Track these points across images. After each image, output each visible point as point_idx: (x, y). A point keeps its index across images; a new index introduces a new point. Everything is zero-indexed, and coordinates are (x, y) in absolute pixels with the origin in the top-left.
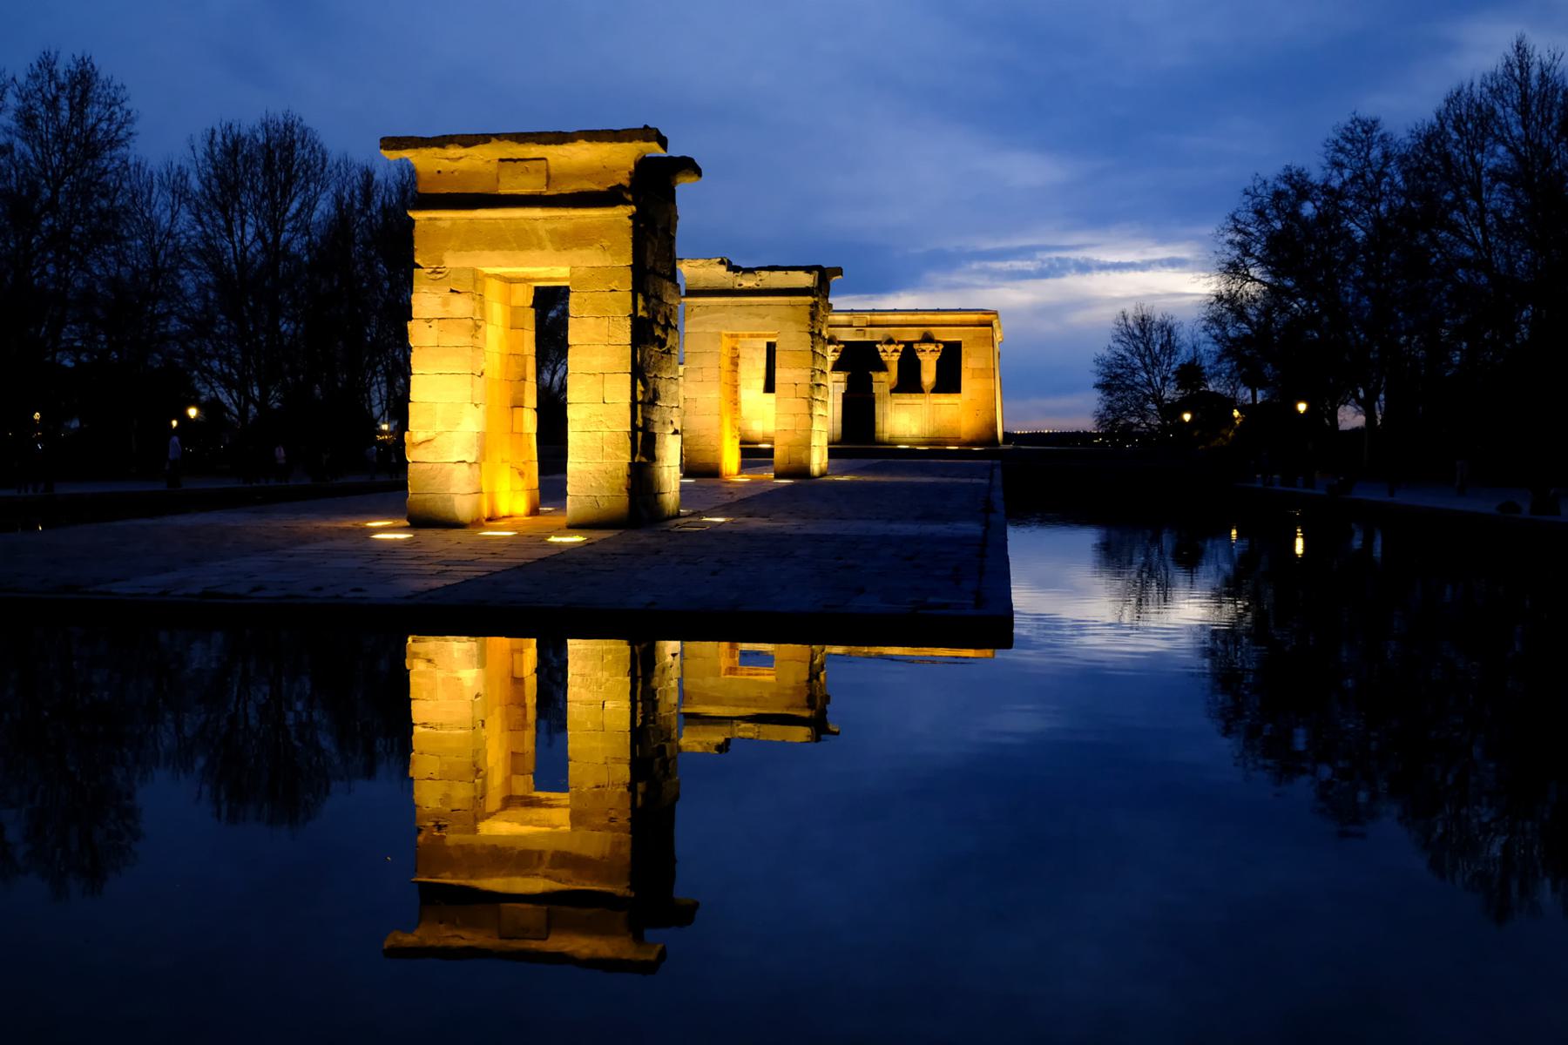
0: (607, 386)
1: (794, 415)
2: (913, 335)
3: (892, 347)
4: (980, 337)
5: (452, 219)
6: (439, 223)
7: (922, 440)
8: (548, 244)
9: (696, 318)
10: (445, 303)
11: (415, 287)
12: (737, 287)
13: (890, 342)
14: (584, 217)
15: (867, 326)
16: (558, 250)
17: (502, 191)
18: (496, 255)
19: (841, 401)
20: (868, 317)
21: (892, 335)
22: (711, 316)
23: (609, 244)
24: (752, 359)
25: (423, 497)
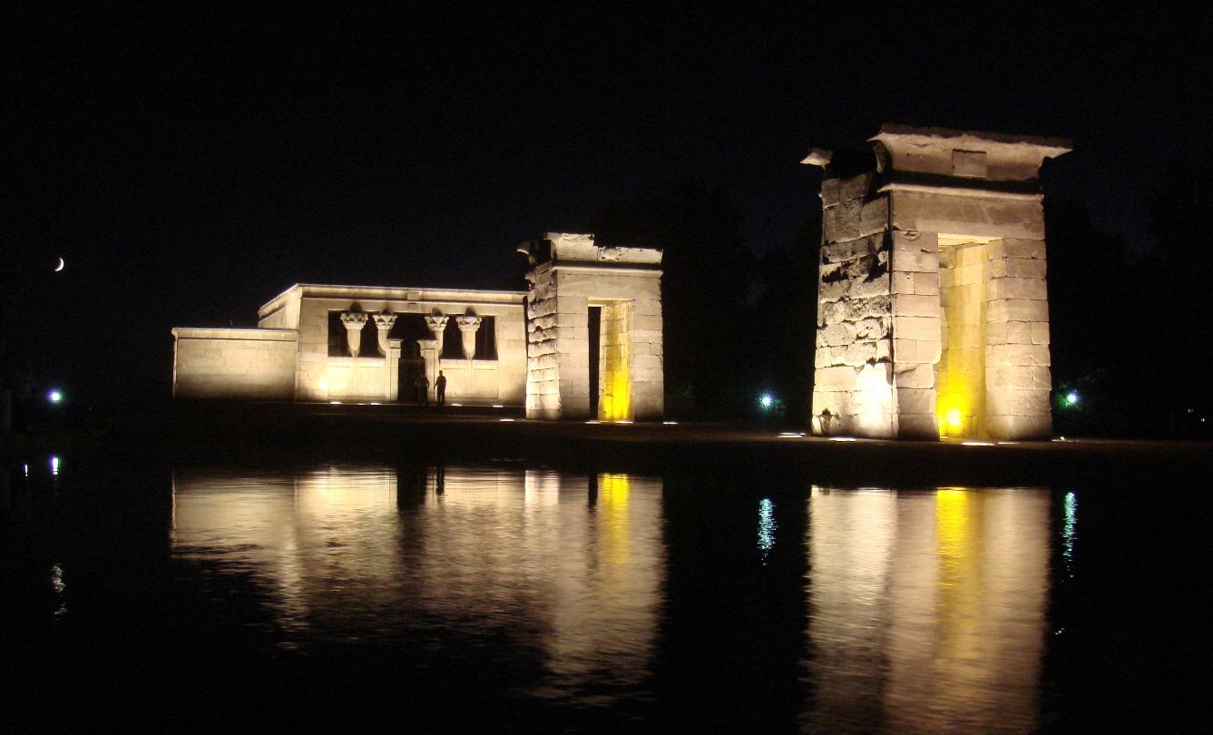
0: (1034, 331)
1: (650, 369)
2: (458, 309)
3: (441, 319)
4: (514, 314)
5: (921, 193)
6: (912, 196)
7: (466, 400)
8: (989, 219)
9: (568, 285)
10: (919, 260)
11: (896, 245)
12: (601, 259)
13: (438, 313)
14: (1011, 200)
15: (420, 300)
16: (995, 224)
17: (958, 173)
18: (954, 226)
19: (397, 365)
20: (421, 293)
21: (440, 309)
22: (580, 283)
23: (1029, 222)
24: (317, 325)
25: (911, 416)
